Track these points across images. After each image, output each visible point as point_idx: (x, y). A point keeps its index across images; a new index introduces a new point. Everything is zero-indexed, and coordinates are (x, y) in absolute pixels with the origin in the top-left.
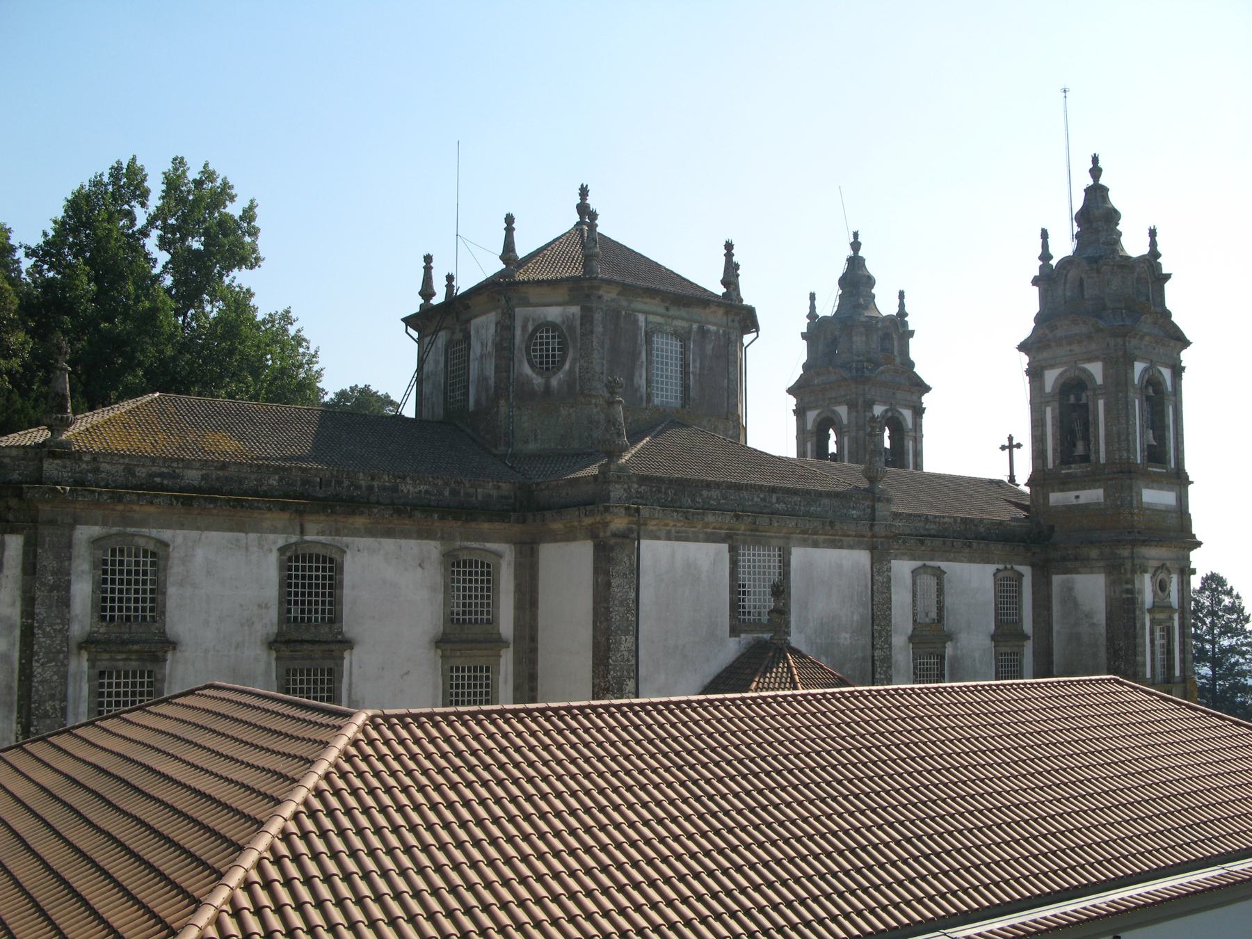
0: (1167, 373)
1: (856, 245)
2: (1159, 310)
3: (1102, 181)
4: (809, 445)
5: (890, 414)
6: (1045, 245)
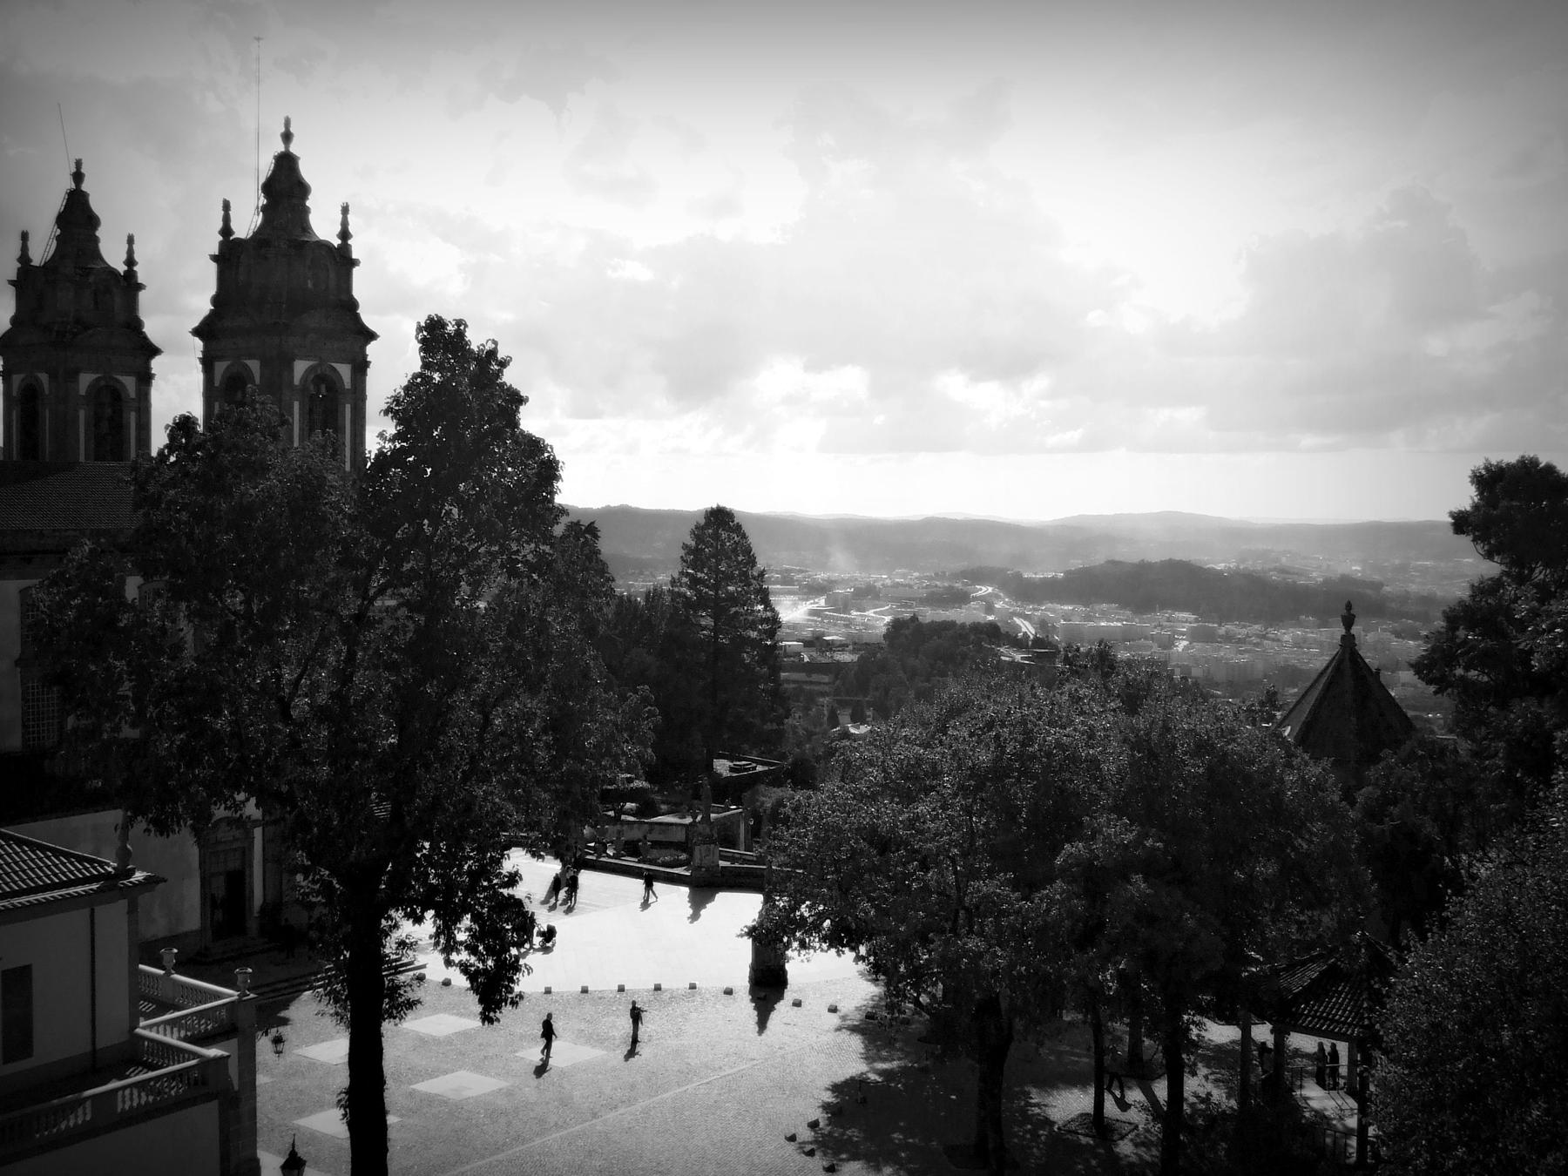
0: (345, 371)
1: (78, 177)
2: (344, 297)
3: (294, 149)
4: (14, 413)
5: (103, 383)
6: (226, 219)
